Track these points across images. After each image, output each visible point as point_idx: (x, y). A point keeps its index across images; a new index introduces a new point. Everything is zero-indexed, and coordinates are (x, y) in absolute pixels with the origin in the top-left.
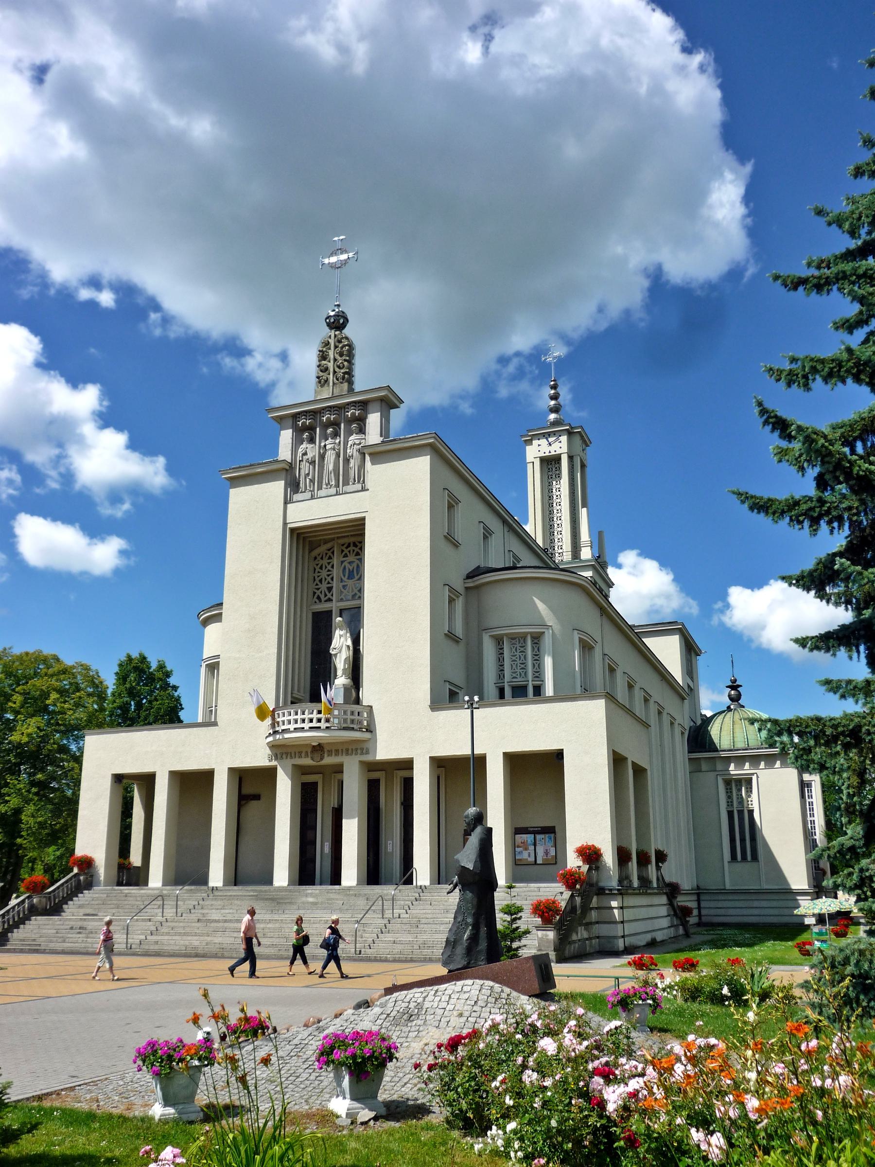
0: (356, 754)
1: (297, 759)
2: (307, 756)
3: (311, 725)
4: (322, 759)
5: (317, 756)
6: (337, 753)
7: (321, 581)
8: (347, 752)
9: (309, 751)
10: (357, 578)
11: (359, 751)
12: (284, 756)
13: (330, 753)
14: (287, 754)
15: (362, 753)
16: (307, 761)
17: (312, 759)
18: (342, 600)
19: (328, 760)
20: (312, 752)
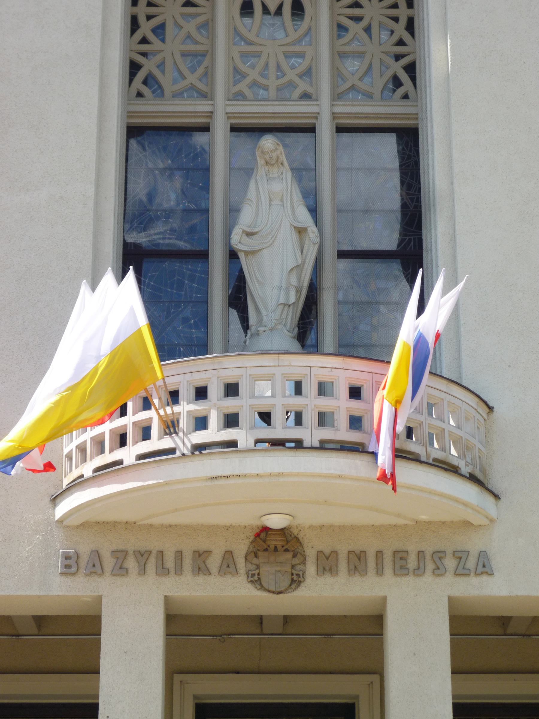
0: (439, 571)
1: (188, 576)
2: (228, 563)
3: (327, 434)
4: (296, 581)
5: (269, 572)
6: (357, 562)
7: (160, 30)
8: (401, 562)
9: (241, 548)
10: (294, 36)
11: (450, 563)
12: (131, 564)
13: (328, 563)
14: (143, 556)
15: (461, 572)
16: (233, 593)
17: (256, 580)
18: (239, 96)
19: (322, 593)
20: (253, 554)
